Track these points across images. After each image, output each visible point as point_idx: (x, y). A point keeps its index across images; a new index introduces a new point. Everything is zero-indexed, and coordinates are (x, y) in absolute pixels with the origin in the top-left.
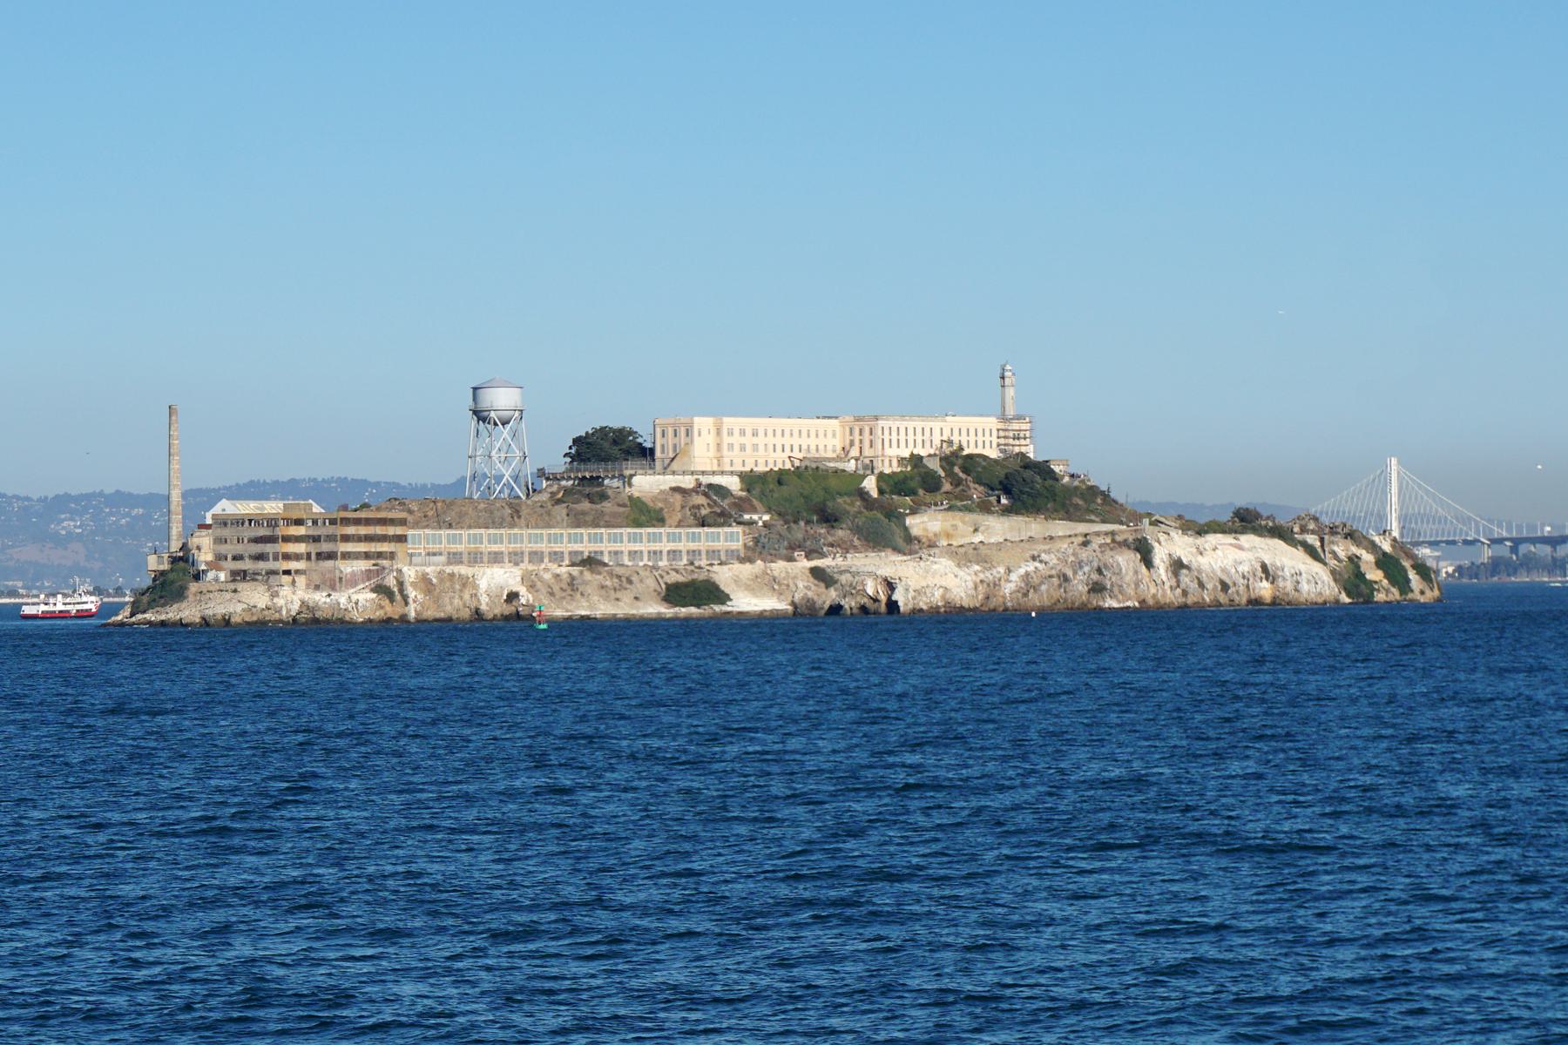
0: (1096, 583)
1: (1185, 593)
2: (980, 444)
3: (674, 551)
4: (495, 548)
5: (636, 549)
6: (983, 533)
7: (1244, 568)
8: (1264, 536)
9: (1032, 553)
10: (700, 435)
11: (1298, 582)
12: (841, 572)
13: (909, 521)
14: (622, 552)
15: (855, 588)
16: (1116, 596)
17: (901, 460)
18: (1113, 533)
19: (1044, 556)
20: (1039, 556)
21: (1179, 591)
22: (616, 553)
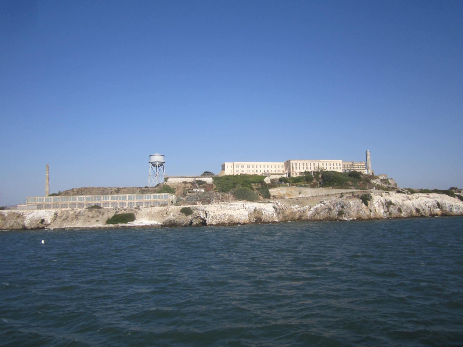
0: (341, 211)
1: (390, 214)
2: (335, 167)
3: (139, 202)
4: (64, 202)
5: (123, 202)
6: (303, 194)
7: (430, 204)
8: (439, 194)
9: (321, 200)
10: (228, 167)
11: (452, 209)
12: (195, 209)
13: (270, 190)
14: (117, 203)
15: (196, 216)
16: (346, 216)
17: (301, 173)
18: (353, 193)
19: (325, 202)
20: (323, 202)
21: (388, 213)
22: (114, 203)
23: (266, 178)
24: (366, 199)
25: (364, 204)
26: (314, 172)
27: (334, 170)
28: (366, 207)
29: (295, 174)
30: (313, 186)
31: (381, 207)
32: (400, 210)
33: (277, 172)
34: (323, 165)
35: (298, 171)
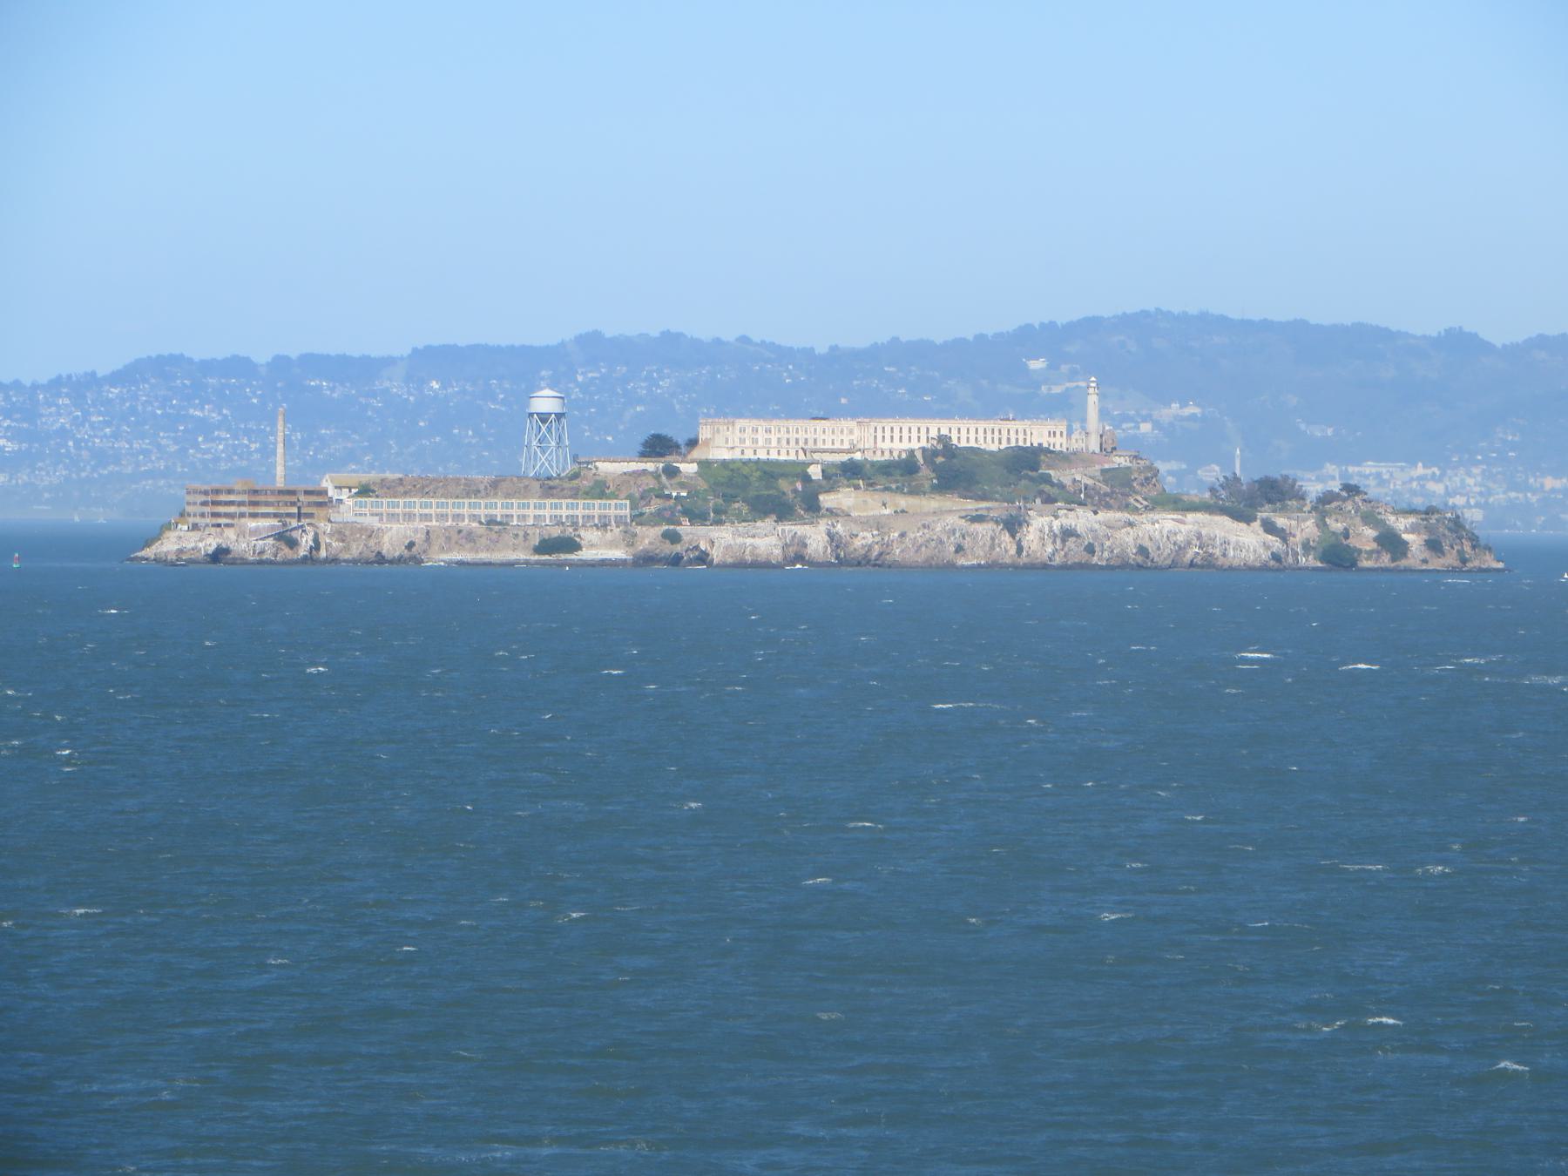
7: (1180, 538)
11: (1226, 550)
13: (821, 498)
23: (812, 467)
24: (1013, 525)
25: (1007, 534)
26: (924, 450)
27: (976, 446)
28: (1011, 539)
29: (879, 453)
30: (915, 492)
31: (1049, 542)
32: (1090, 549)
33: (837, 446)
34: (950, 432)
35: (887, 445)
